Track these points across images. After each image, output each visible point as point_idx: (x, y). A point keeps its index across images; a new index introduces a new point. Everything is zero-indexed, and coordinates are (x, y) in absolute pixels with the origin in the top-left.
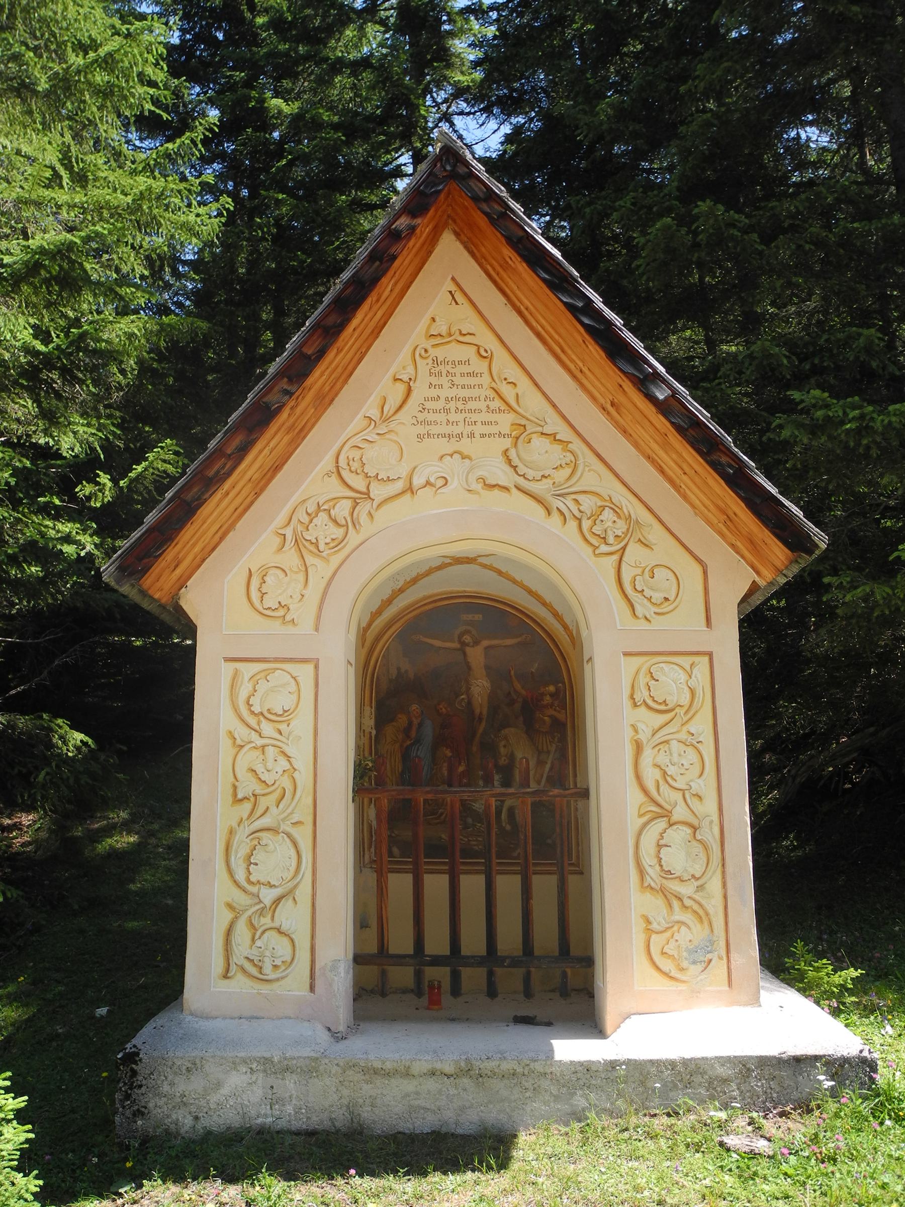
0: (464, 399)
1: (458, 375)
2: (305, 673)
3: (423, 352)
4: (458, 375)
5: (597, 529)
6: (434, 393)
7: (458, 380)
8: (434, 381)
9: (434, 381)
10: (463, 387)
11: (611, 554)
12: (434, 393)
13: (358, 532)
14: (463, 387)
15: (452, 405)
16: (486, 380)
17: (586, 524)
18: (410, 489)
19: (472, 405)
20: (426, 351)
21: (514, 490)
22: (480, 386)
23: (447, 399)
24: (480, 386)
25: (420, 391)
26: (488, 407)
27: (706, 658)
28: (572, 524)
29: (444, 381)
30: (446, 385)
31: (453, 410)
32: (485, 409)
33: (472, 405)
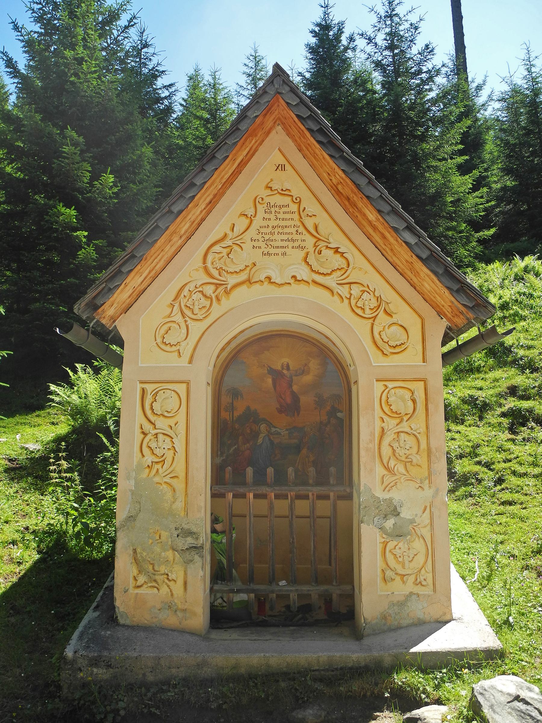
1: (282, 213)
3: (260, 199)
4: (282, 213)
5: (360, 304)
6: (265, 223)
7: (279, 216)
8: (267, 216)
9: (267, 216)
10: (283, 219)
11: (370, 318)
12: (265, 223)
14: (283, 219)
15: (276, 231)
16: (296, 216)
17: (353, 302)
18: (249, 281)
19: (286, 230)
20: (262, 199)
21: (310, 281)
22: (292, 219)
23: (273, 227)
24: (292, 219)
25: (258, 222)
27: (423, 383)
28: (346, 301)
29: (272, 216)
31: (276, 233)
32: (295, 233)
33: (286, 230)
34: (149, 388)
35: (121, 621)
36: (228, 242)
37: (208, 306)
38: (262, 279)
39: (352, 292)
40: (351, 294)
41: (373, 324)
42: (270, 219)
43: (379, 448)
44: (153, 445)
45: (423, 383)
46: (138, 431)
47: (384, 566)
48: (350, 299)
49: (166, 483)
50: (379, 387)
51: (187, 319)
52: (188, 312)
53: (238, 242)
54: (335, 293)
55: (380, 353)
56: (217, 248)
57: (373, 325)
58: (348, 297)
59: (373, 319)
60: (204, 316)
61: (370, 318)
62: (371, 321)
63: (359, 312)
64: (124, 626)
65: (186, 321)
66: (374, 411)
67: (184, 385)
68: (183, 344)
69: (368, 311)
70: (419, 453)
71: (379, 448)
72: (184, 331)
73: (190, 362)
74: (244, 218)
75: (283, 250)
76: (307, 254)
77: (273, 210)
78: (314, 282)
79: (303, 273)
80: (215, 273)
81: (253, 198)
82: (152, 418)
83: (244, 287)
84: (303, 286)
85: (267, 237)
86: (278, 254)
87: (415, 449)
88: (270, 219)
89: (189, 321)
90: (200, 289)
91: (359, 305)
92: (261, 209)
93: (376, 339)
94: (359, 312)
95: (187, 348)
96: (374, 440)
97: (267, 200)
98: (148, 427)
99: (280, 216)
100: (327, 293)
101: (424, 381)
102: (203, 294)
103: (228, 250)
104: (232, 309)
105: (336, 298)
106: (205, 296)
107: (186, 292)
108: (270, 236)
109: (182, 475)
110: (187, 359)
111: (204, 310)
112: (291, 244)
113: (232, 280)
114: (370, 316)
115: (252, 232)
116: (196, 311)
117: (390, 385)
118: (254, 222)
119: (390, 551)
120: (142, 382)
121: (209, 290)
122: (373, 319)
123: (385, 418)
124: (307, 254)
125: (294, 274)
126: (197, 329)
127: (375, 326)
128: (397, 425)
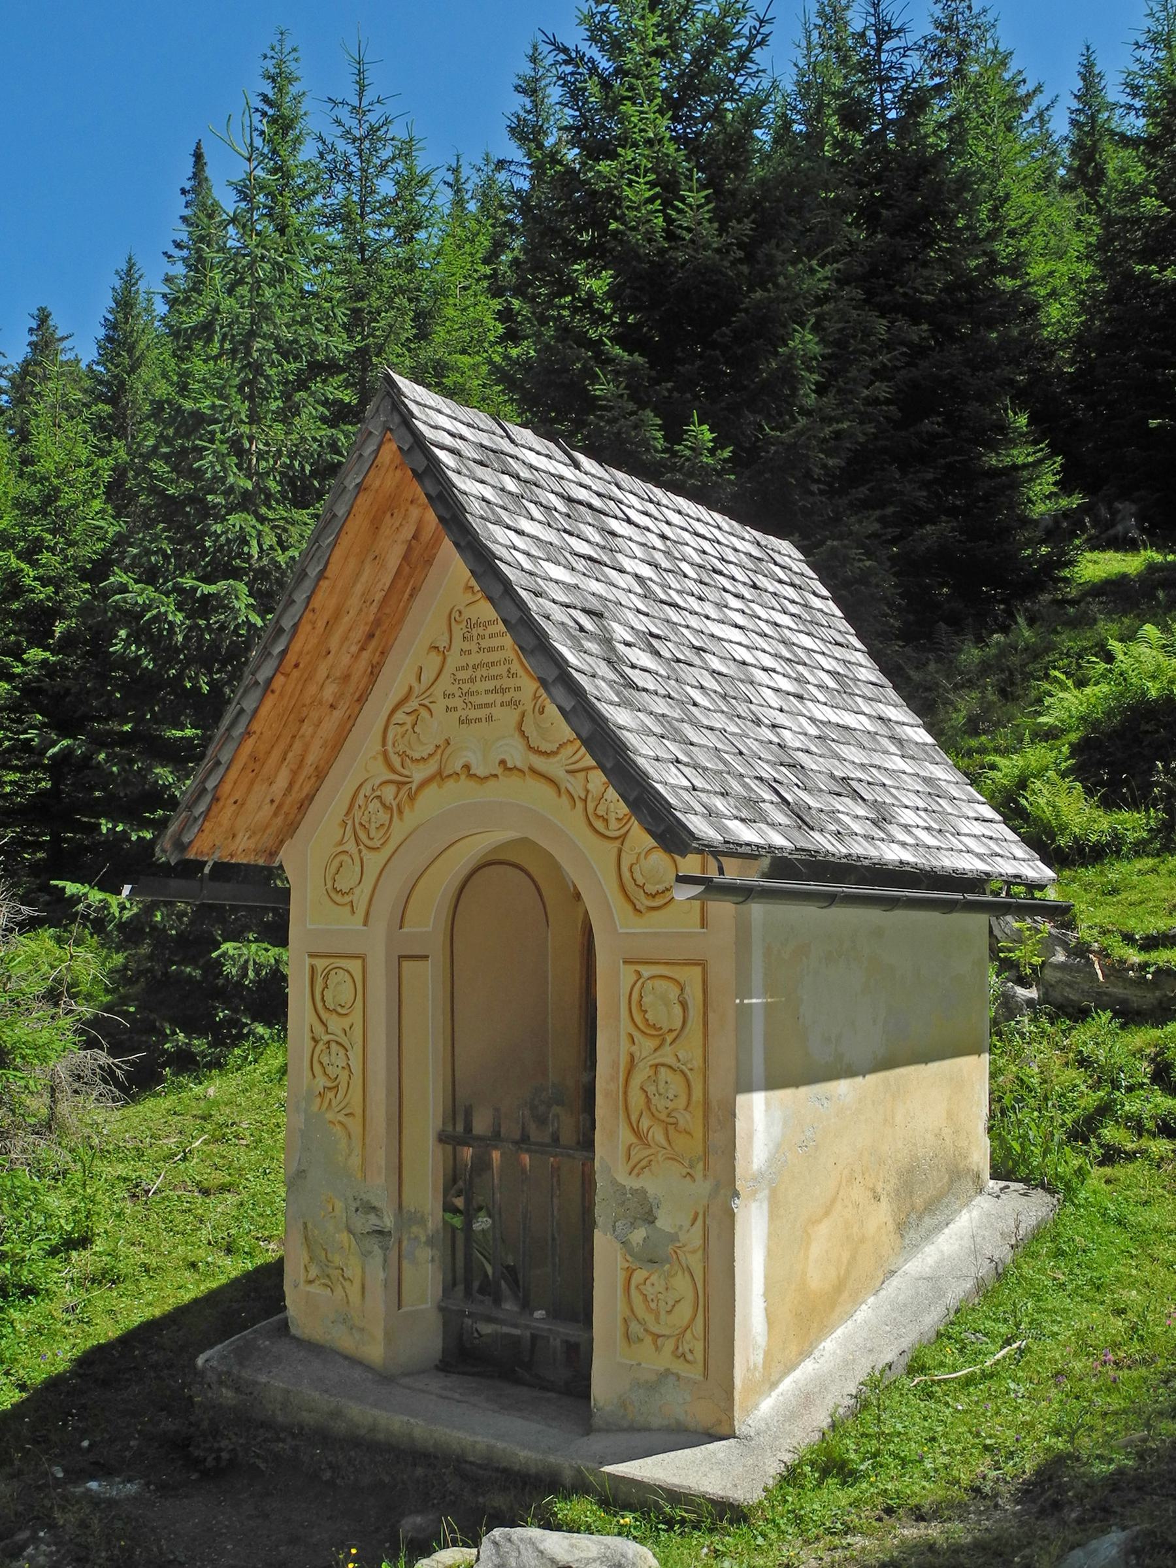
0: (488, 665)
2: (355, 966)
8: (466, 646)
9: (466, 646)
13: (401, 819)
15: (479, 673)
17: (591, 806)
18: (440, 776)
19: (494, 671)
21: (526, 770)
22: (502, 648)
24: (502, 648)
25: (454, 660)
26: (509, 671)
27: (698, 970)
28: (580, 805)
29: (473, 646)
30: (474, 648)
32: (505, 674)
33: (494, 671)
34: (320, 964)
35: (293, 1331)
36: (413, 704)
37: (387, 823)
38: (458, 769)
39: (590, 786)
40: (588, 791)
41: (620, 851)
42: (470, 652)
43: (625, 1093)
44: (325, 1060)
45: (698, 970)
46: (307, 1036)
47: (628, 1313)
48: (585, 801)
49: (340, 1122)
50: (627, 975)
51: (362, 847)
52: (362, 835)
53: (426, 702)
54: (563, 790)
55: (629, 908)
56: (400, 716)
57: (620, 851)
58: (583, 797)
59: (620, 841)
60: (381, 841)
61: (616, 838)
62: (617, 844)
63: (599, 825)
64: (294, 1338)
65: (360, 851)
66: (619, 1021)
67: (359, 962)
68: (357, 891)
69: (613, 824)
70: (690, 1109)
71: (625, 1093)
72: (358, 869)
73: (365, 924)
74: (434, 654)
75: (487, 711)
76: (523, 715)
77: (475, 632)
78: (533, 770)
79: (517, 755)
80: (396, 761)
81: (448, 611)
82: (324, 1015)
83: (434, 786)
84: (515, 780)
85: (465, 687)
86: (480, 720)
87: (682, 1101)
88: (470, 652)
89: (364, 851)
90: (378, 793)
91: (600, 813)
92: (458, 631)
93: (624, 880)
94: (599, 825)
95: (361, 897)
96: (618, 1079)
97: (467, 614)
98: (319, 1029)
99: (485, 643)
100: (548, 791)
101: (702, 964)
102: (381, 802)
103: (414, 717)
104: (415, 830)
105: (565, 799)
106: (384, 805)
107: (360, 800)
108: (470, 685)
109: (358, 1111)
110: (361, 920)
111: (382, 831)
112: (498, 698)
113: (418, 774)
114: (617, 834)
115: (445, 683)
116: (373, 834)
117: (646, 971)
118: (449, 660)
119: (637, 1287)
120: (311, 956)
121: (389, 793)
122: (620, 841)
123: (636, 1034)
124: (523, 715)
125: (502, 757)
126: (374, 861)
127: (623, 855)
128: (656, 1050)
